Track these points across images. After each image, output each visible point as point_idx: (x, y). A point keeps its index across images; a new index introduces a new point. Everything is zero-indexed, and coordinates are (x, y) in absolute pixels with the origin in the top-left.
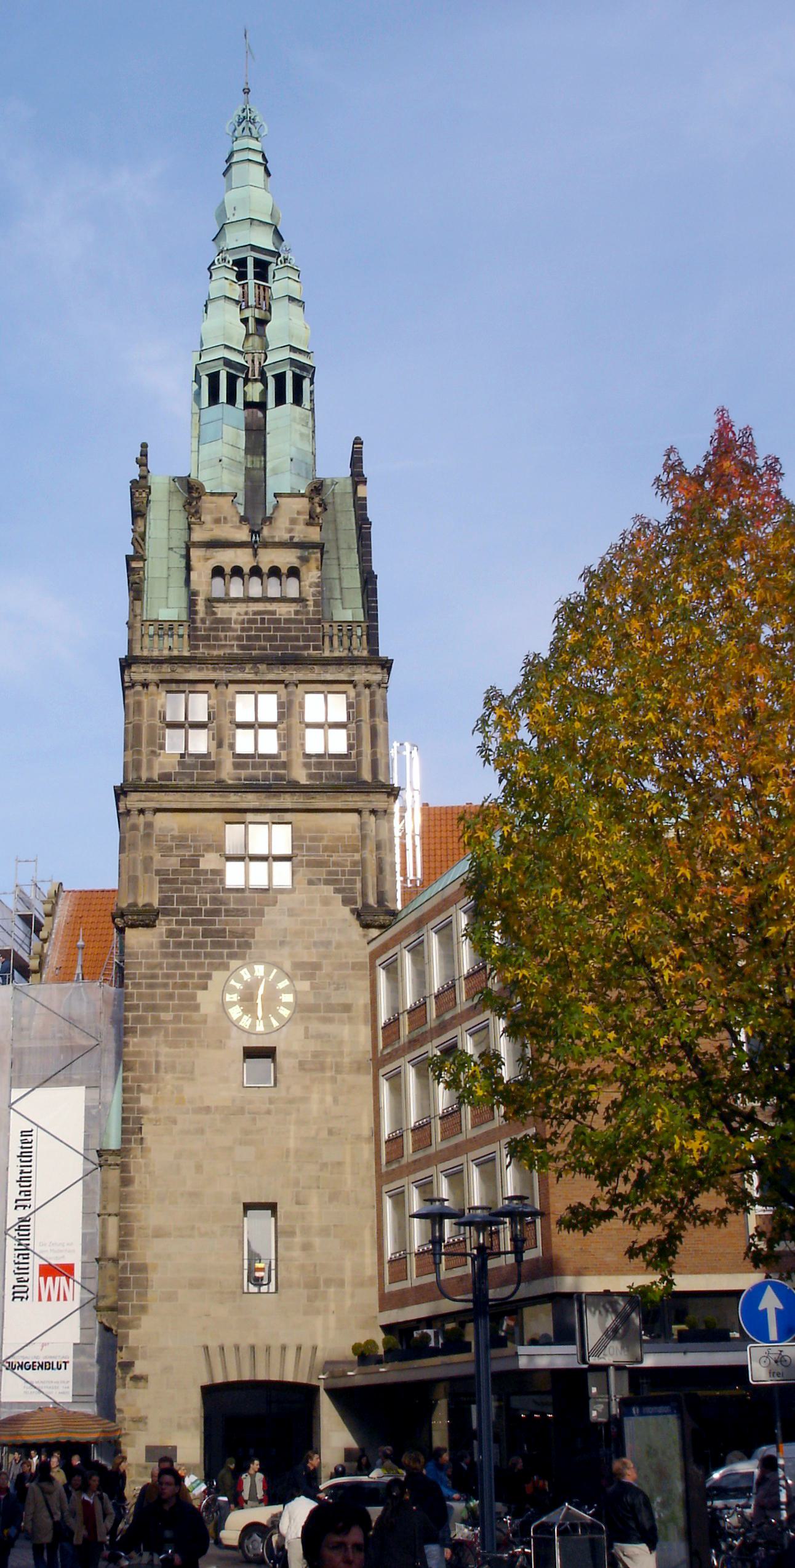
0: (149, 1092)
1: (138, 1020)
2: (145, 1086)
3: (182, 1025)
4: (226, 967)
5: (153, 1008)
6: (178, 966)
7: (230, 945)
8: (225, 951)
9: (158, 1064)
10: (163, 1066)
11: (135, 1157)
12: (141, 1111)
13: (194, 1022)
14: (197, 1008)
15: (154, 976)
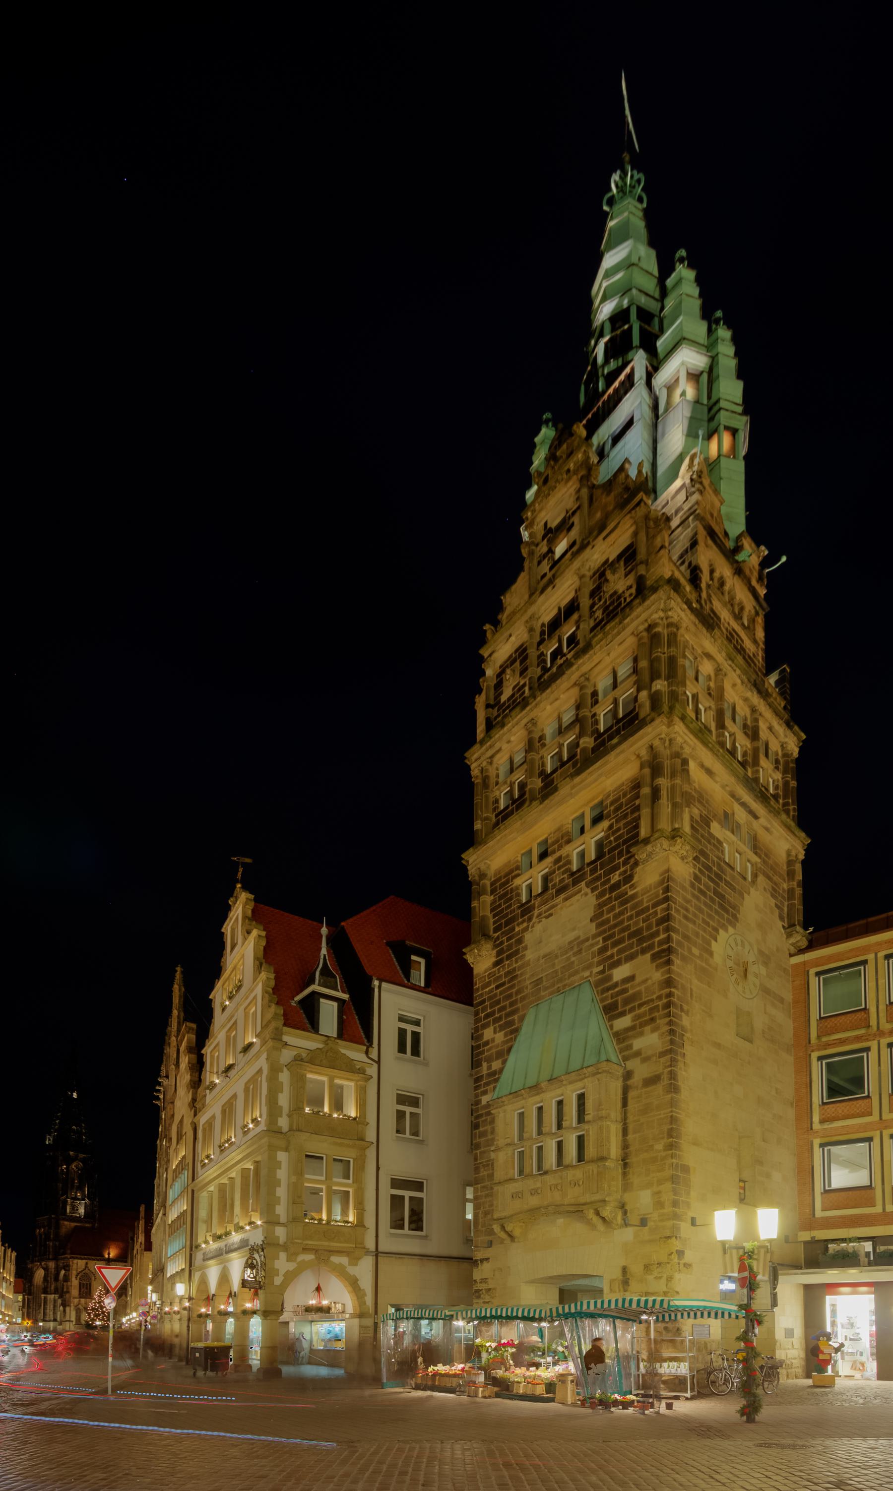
0: (687, 1014)
1: (679, 944)
2: (685, 1007)
3: (704, 965)
4: (726, 930)
5: (686, 937)
6: (701, 911)
7: (727, 911)
8: (726, 915)
9: (691, 989)
10: (694, 995)
11: (680, 1069)
12: (683, 1028)
13: (710, 965)
14: (711, 954)
15: (687, 910)
